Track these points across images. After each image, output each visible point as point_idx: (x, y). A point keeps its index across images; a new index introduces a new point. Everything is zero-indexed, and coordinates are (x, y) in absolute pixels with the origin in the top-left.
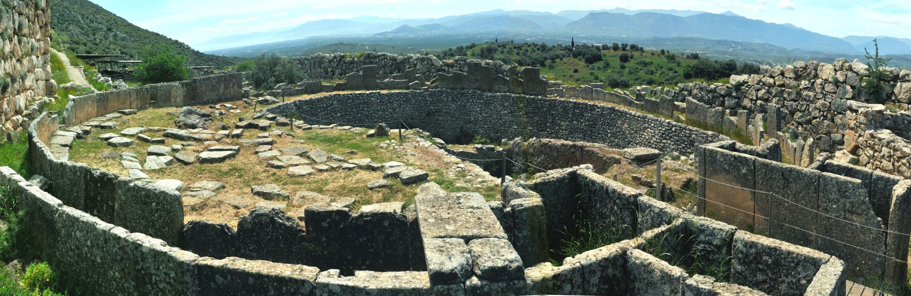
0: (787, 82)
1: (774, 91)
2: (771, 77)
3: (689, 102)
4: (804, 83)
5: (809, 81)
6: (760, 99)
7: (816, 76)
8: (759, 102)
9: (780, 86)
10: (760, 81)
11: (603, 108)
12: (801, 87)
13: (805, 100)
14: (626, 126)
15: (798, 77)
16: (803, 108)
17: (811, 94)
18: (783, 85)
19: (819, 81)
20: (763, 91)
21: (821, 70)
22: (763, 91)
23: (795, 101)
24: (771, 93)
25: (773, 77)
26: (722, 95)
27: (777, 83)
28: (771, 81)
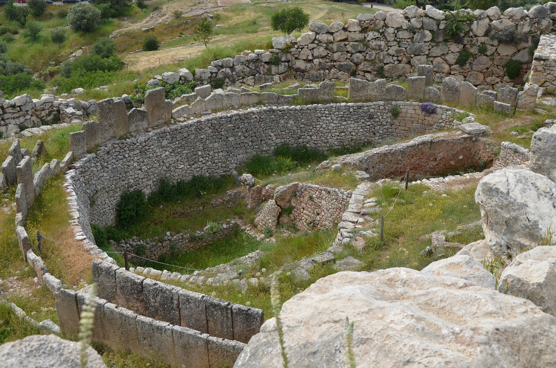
0: (352, 35)
1: (335, 47)
2: (328, 33)
3: (353, 82)
4: (371, 35)
5: (379, 32)
6: (317, 57)
7: (386, 26)
8: (316, 61)
9: (340, 41)
10: (315, 39)
11: (260, 113)
12: (368, 39)
13: (373, 49)
14: (291, 122)
15: (364, 30)
16: (373, 58)
17: (383, 43)
18: (346, 40)
19: (391, 30)
20: (322, 49)
21: (392, 19)
22: (322, 49)
23: (360, 52)
24: (331, 50)
25: (332, 34)
26: (266, 63)
27: (339, 39)
28: (331, 38)
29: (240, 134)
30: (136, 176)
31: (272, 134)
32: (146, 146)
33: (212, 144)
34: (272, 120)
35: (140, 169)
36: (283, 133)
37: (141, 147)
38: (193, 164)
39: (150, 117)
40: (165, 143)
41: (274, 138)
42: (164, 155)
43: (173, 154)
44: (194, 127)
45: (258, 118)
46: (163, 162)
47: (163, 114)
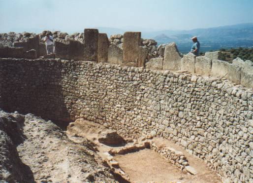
29: (170, 100)
30: (85, 92)
31: (198, 118)
32: (99, 73)
33: (147, 99)
34: (204, 98)
35: (89, 89)
36: (210, 123)
37: (95, 71)
38: (129, 110)
39: (124, 57)
40: (113, 78)
41: (199, 124)
42: (109, 87)
43: (115, 90)
44: (141, 75)
45: (192, 89)
46: (106, 92)
47: (135, 58)
